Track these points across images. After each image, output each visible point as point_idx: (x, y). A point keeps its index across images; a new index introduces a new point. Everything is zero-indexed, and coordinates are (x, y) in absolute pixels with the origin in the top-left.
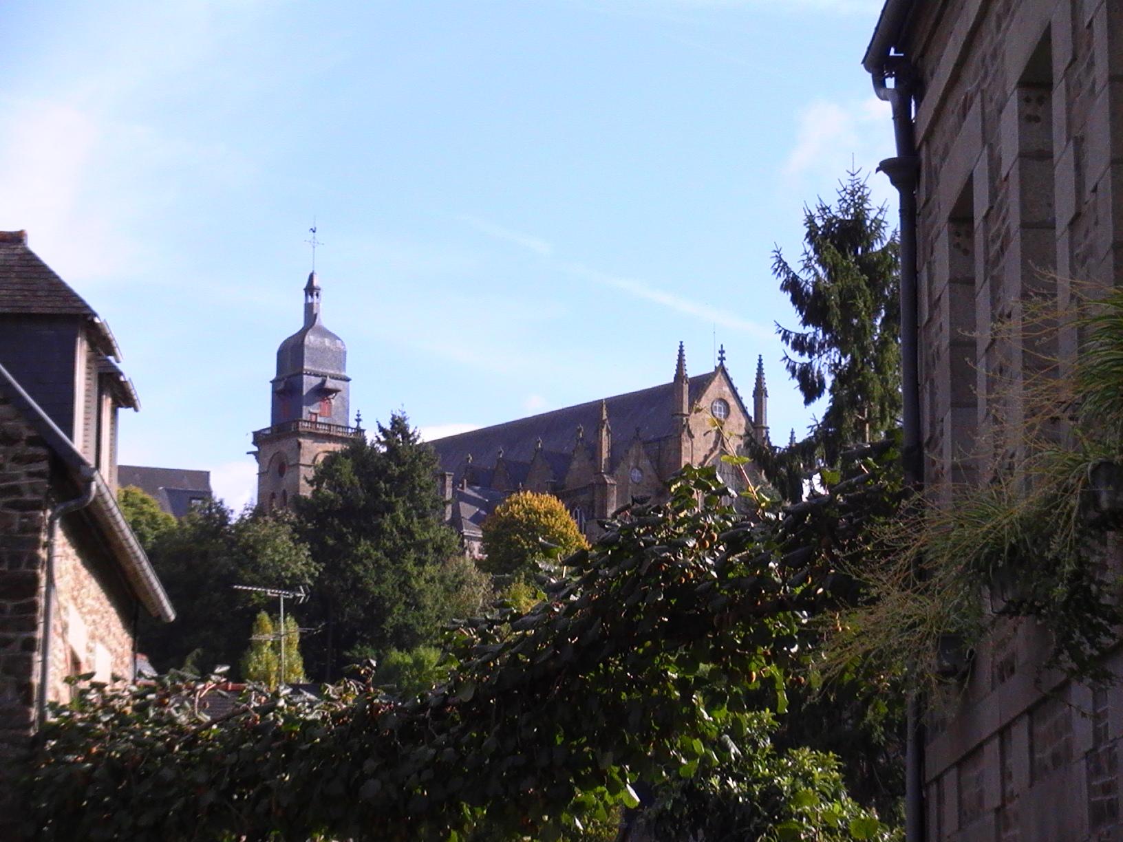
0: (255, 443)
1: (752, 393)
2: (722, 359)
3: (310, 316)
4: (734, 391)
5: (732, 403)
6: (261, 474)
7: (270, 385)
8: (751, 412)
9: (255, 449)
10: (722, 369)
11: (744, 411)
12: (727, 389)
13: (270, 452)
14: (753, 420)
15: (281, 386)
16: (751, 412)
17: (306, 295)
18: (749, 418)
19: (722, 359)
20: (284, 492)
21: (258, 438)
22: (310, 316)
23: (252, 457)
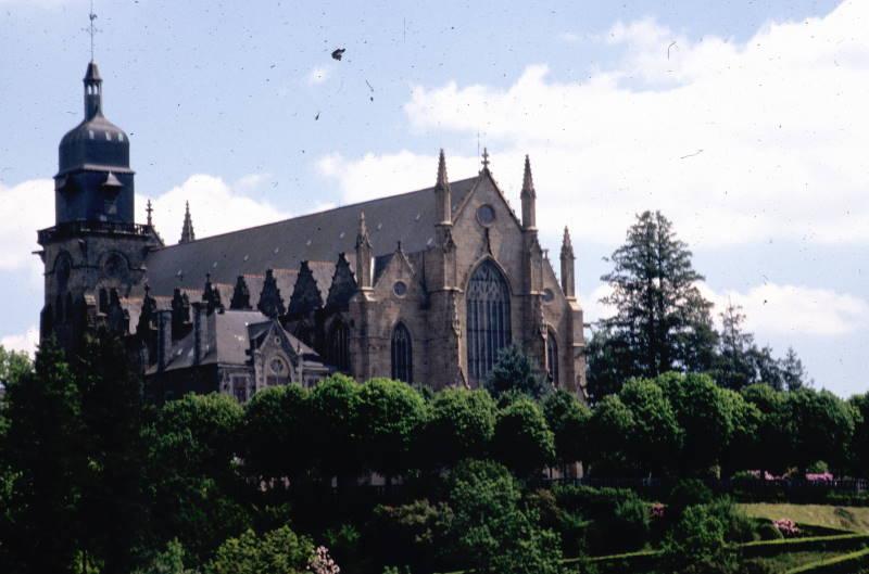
0: (41, 241)
1: (519, 195)
2: (486, 163)
3: (93, 107)
4: (499, 195)
5: (498, 207)
6: (46, 275)
8: (519, 215)
9: (41, 248)
10: (486, 174)
11: (512, 214)
12: (492, 194)
13: (54, 249)
14: (521, 223)
16: (519, 215)
17: (86, 86)
18: (516, 221)
19: (486, 163)
21: (45, 237)
22: (93, 107)
23: (38, 257)
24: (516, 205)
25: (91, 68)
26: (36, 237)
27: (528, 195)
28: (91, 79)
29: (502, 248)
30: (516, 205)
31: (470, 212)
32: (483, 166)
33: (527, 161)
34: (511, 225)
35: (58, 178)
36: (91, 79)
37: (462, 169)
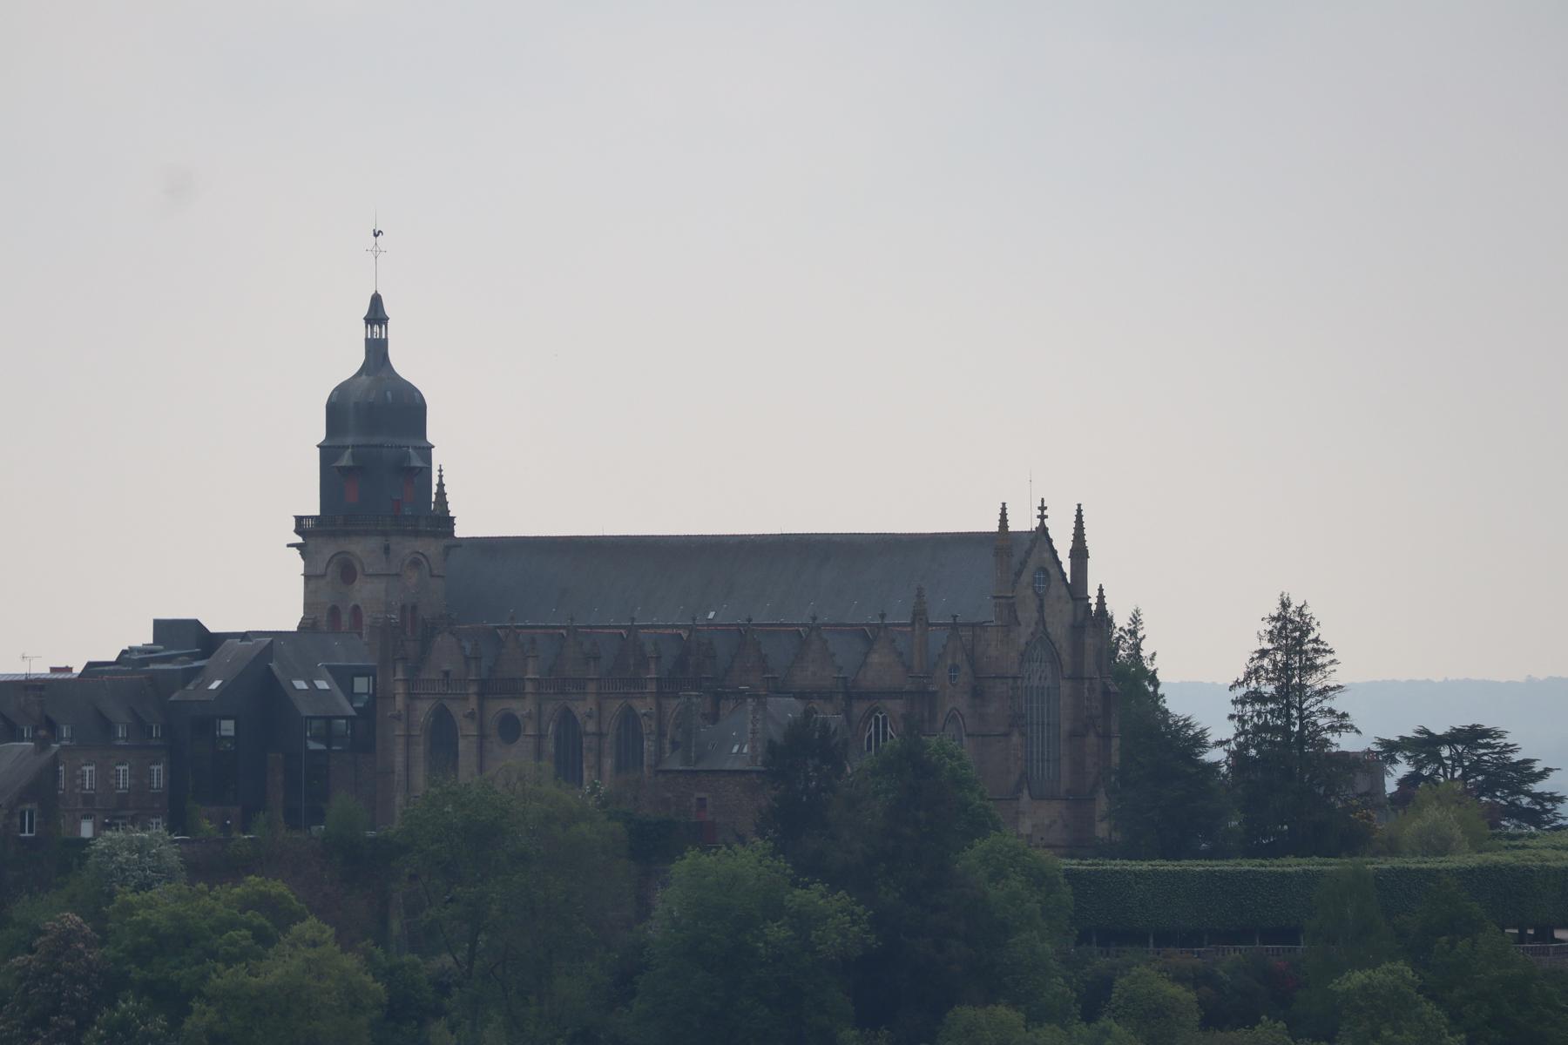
0: (298, 531)
2: (1043, 517)
3: (377, 351)
4: (1054, 553)
5: (1053, 571)
6: (308, 577)
7: (316, 454)
9: (299, 540)
10: (1043, 530)
12: (1047, 555)
13: (329, 549)
15: (346, 460)
19: (1043, 517)
20: (356, 608)
22: (377, 351)
23: (295, 552)
24: (1067, 567)
25: (376, 301)
26: (292, 524)
27: (1080, 552)
28: (376, 315)
29: (1058, 627)
30: (1067, 567)
31: (1026, 578)
32: (1037, 522)
33: (1079, 511)
34: (1064, 590)
35: (328, 453)
36: (376, 315)
37: (1022, 522)
